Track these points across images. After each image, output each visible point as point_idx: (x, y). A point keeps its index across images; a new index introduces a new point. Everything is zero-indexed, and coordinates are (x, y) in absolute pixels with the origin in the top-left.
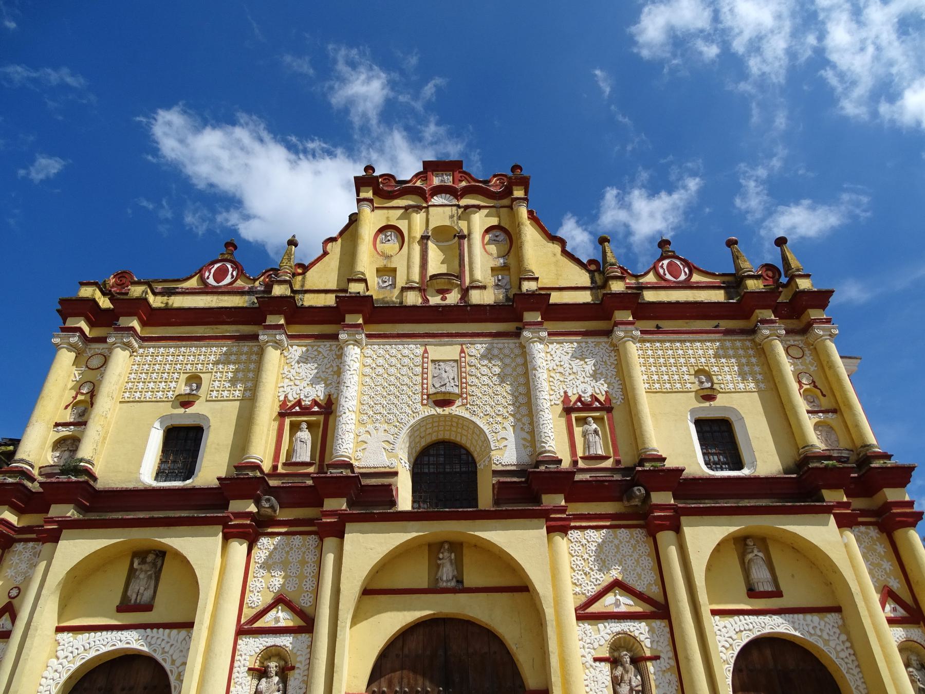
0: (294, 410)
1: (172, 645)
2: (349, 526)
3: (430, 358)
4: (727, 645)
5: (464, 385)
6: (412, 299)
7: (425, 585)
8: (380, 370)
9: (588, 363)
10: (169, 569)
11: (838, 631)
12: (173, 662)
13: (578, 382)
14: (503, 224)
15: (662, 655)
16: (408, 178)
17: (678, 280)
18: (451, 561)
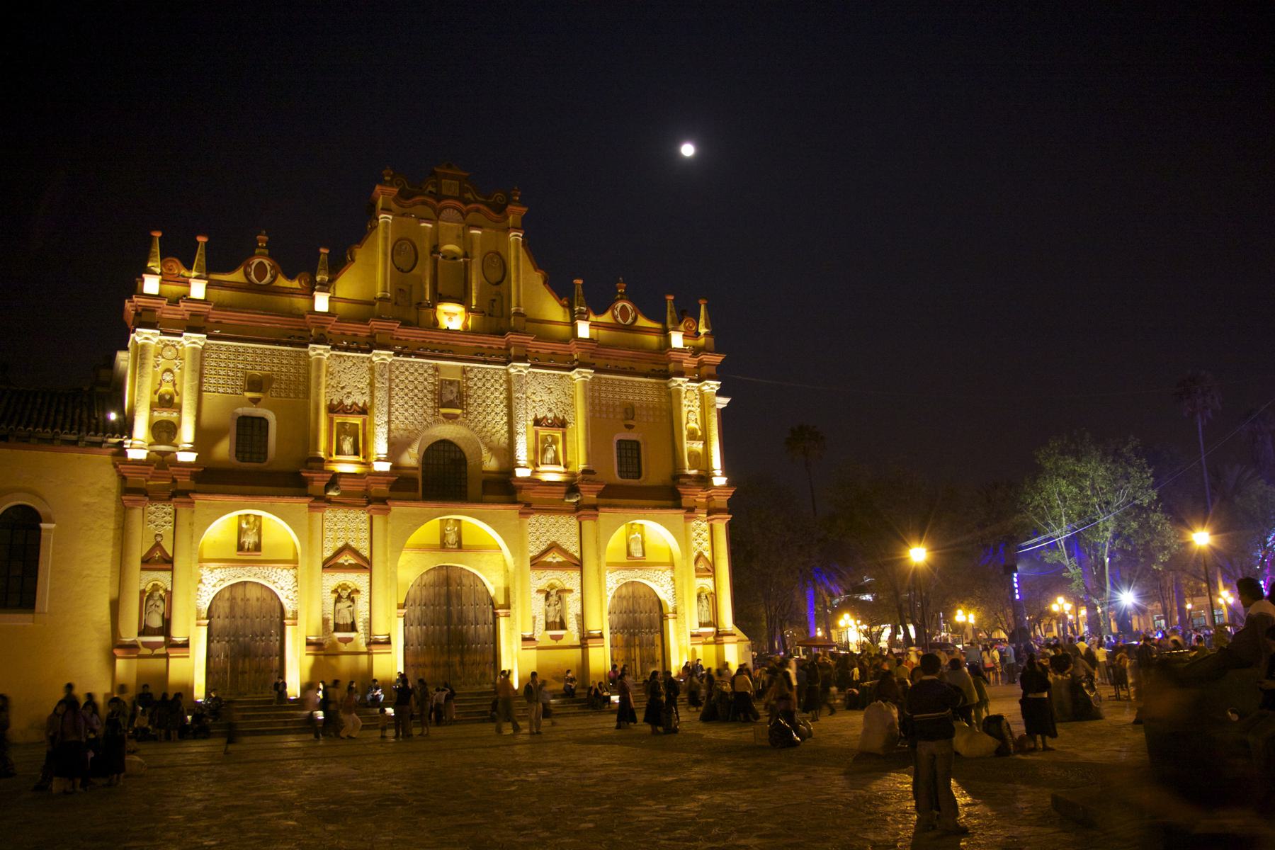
1: (279, 579)
14: (500, 251)
17: (627, 323)
18: (455, 532)
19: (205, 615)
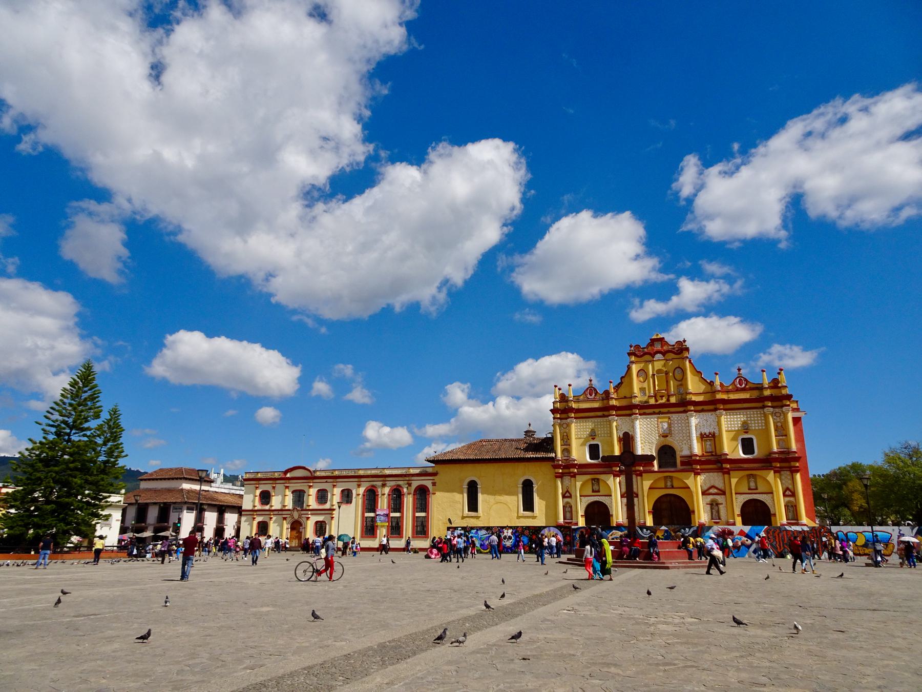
2: (643, 474)
6: (652, 401)
7: (663, 486)
8: (645, 426)
10: (601, 484)
16: (645, 346)
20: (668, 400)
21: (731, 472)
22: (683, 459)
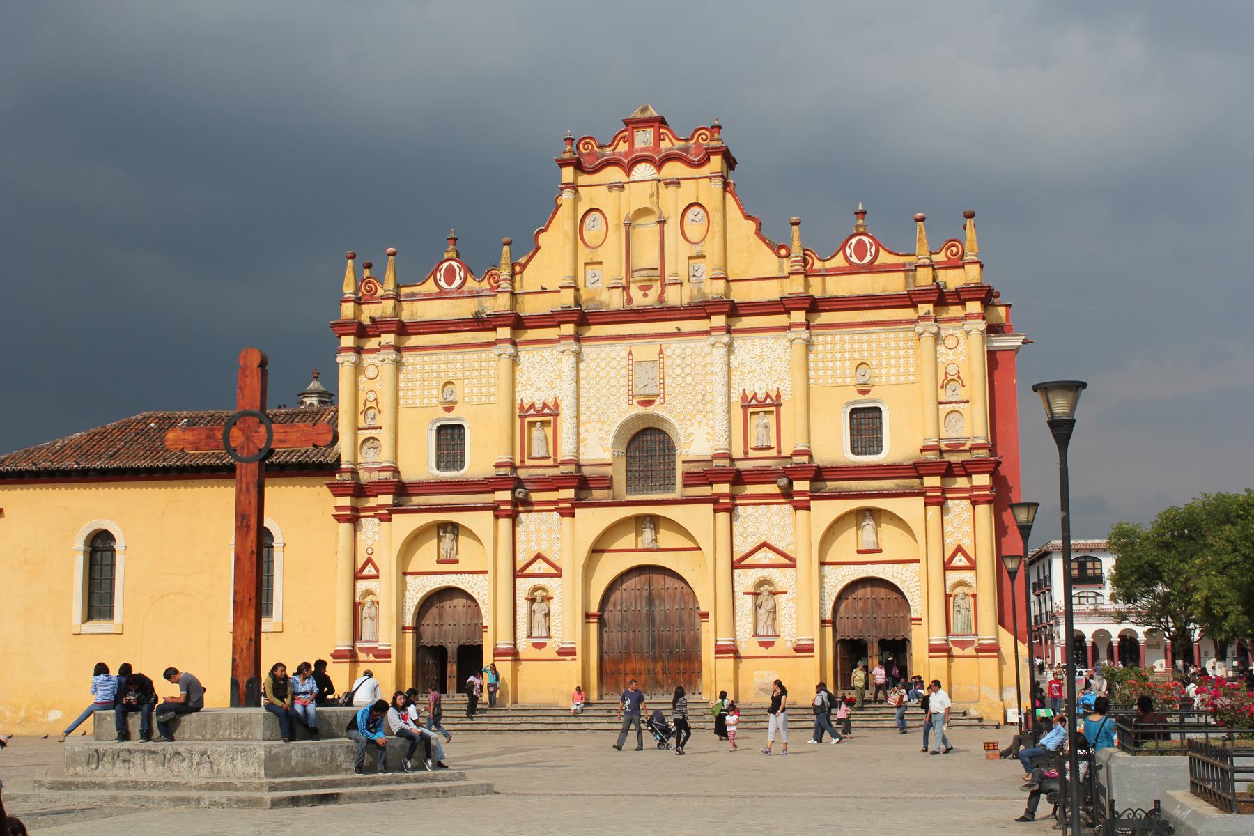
0: (530, 413)
3: (634, 361)
4: (834, 584)
5: (662, 385)
6: (615, 301)
9: (766, 360)
11: (913, 574)
12: (478, 593)
13: (756, 380)
15: (789, 591)
17: (863, 262)
19: (409, 621)
20: (661, 298)
21: (813, 504)
22: (686, 465)
